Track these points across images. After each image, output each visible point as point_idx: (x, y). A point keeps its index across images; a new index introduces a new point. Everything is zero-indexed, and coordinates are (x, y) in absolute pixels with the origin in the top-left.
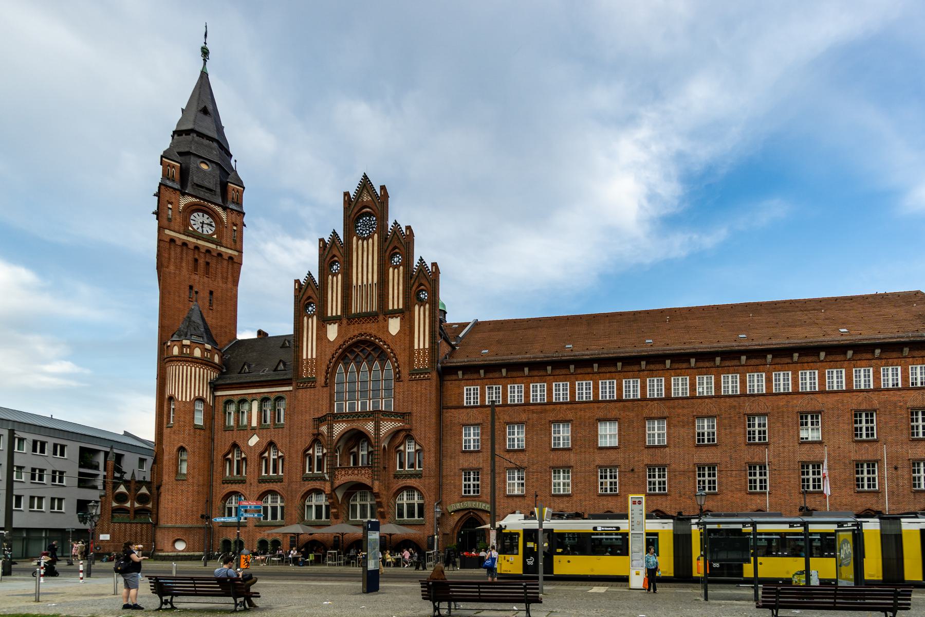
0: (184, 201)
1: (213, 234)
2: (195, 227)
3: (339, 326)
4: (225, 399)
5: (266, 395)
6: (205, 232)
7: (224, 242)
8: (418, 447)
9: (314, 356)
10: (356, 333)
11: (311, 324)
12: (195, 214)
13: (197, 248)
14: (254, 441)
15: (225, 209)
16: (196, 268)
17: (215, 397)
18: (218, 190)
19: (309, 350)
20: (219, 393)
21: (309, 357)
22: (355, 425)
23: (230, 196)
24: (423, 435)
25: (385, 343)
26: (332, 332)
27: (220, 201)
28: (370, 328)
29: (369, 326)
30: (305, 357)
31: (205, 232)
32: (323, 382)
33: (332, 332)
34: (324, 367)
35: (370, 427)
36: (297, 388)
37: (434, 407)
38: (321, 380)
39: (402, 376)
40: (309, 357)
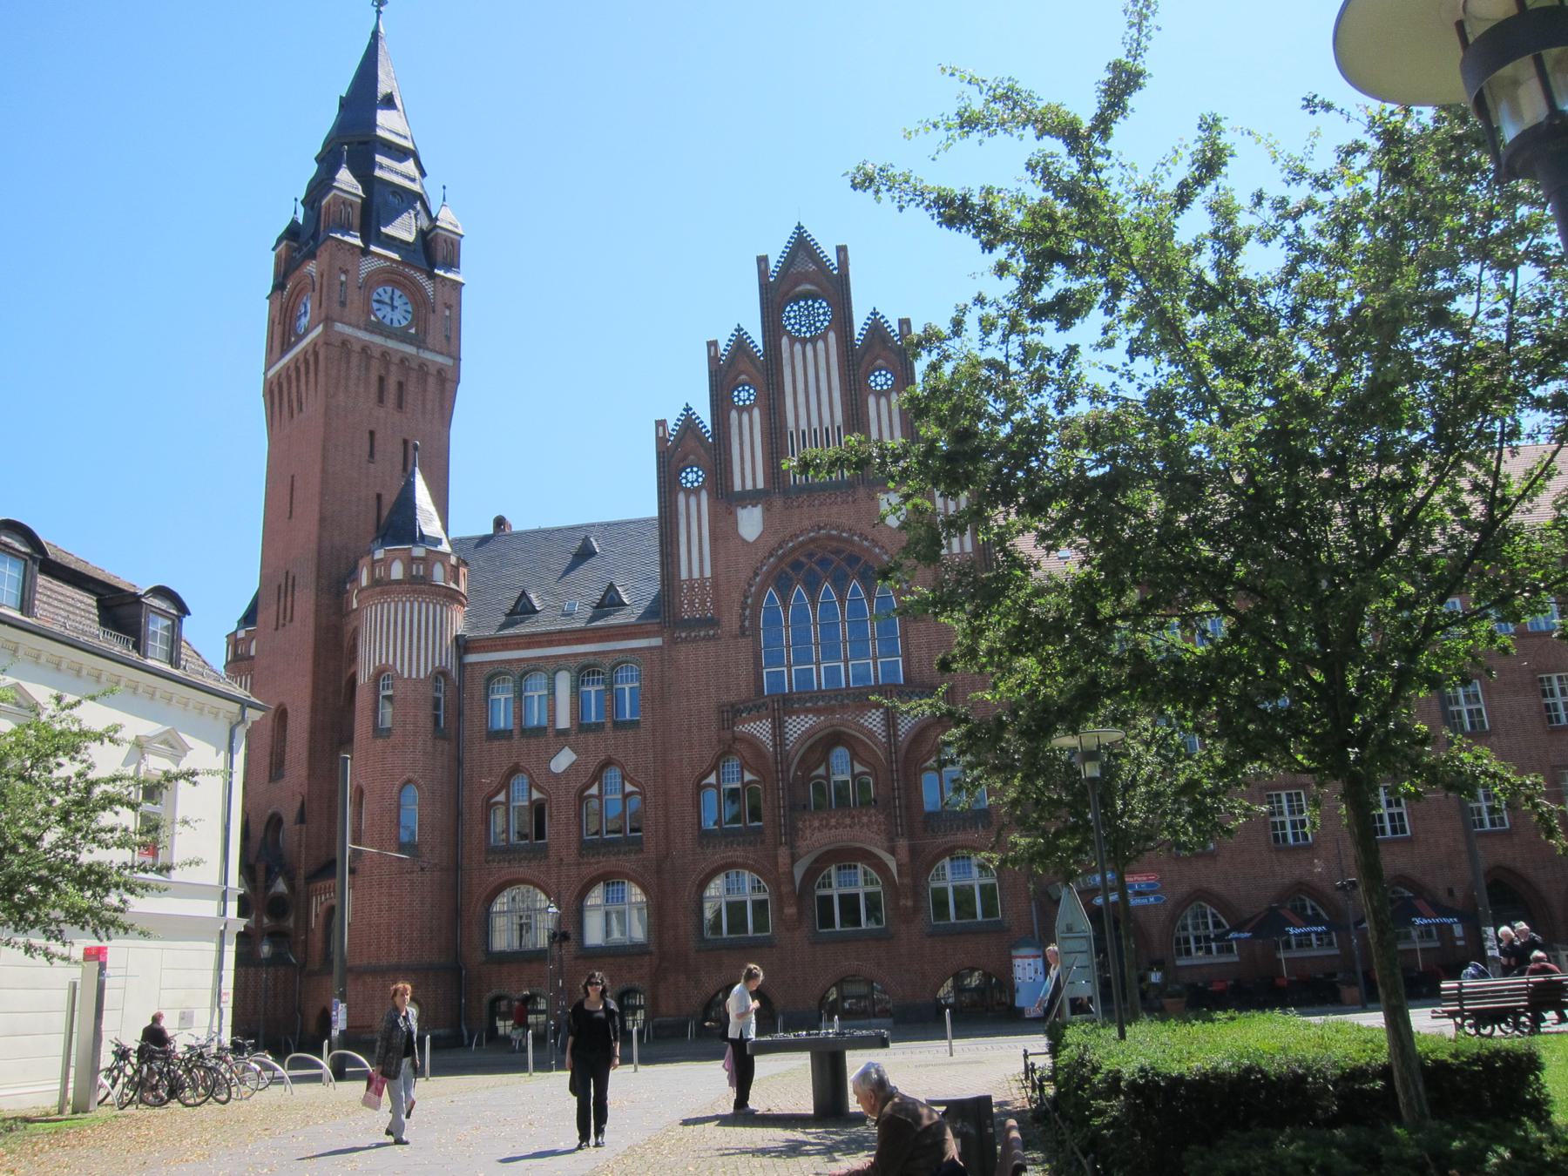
3: (767, 510)
4: (488, 670)
5: (591, 659)
6: (396, 324)
9: (708, 574)
10: (806, 523)
13: (385, 354)
14: (563, 760)
16: (381, 400)
17: (462, 666)
20: (472, 658)
21: (696, 575)
25: (875, 542)
26: (750, 523)
28: (839, 516)
29: (835, 509)
30: (684, 575)
31: (396, 324)
32: (735, 626)
33: (750, 523)
34: (737, 596)
36: (673, 642)
38: (731, 621)
40: (696, 575)
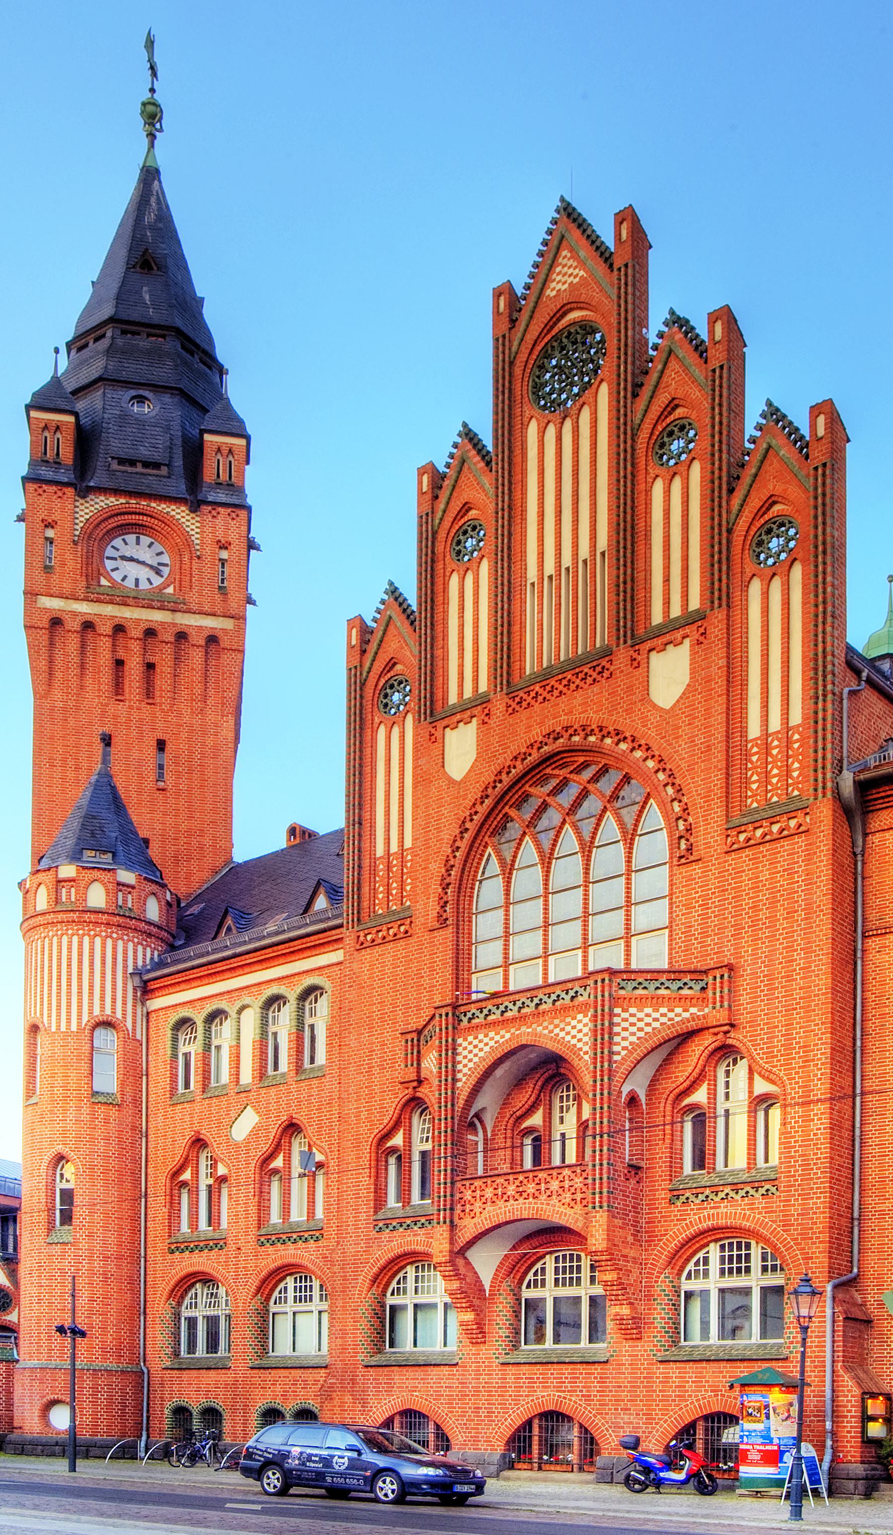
0: (90, 508)
1: (165, 586)
2: (117, 576)
7: (193, 599)
8: (762, 1087)
11: (396, 743)
12: (118, 542)
15: (196, 505)
18: (178, 462)
19: (396, 827)
22: (525, 1033)
23: (209, 475)
24: (779, 1042)
27: (180, 487)
35: (573, 1035)
37: (823, 927)
39: (700, 840)
